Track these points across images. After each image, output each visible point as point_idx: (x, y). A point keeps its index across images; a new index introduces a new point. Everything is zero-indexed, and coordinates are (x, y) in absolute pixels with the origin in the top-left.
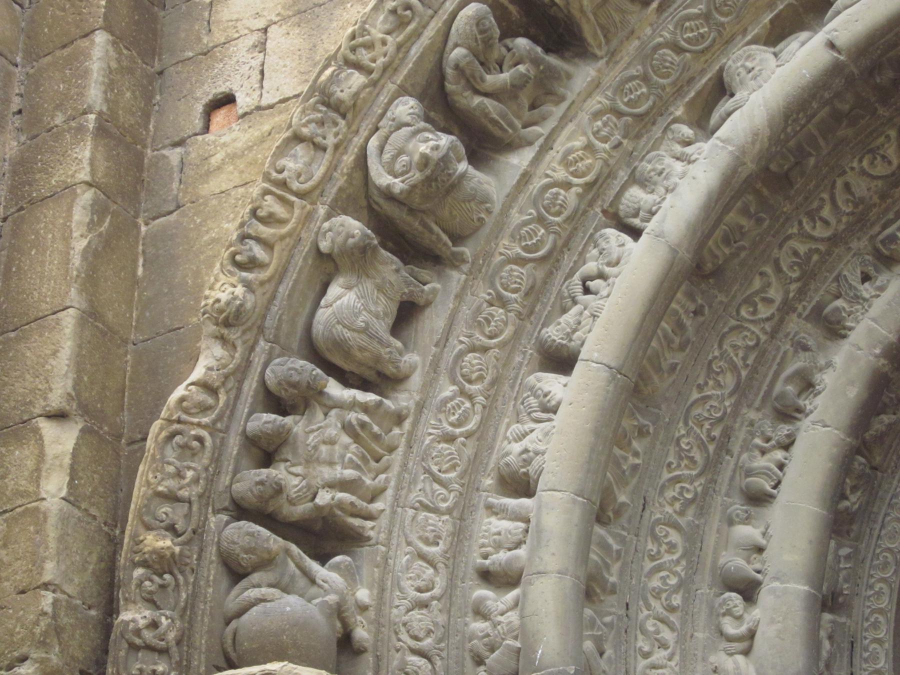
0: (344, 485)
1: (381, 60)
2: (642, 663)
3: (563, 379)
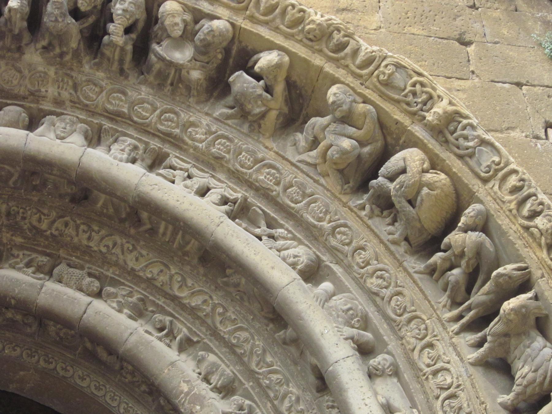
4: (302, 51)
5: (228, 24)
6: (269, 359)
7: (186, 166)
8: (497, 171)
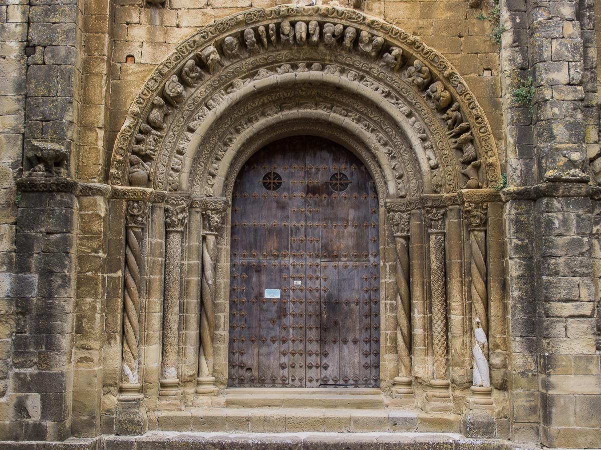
0: (152, 150)
1: (172, 66)
2: (195, 187)
3: (192, 134)
4: (406, 48)
5: (383, 40)
6: (397, 138)
7: (371, 80)
8: (463, 93)
